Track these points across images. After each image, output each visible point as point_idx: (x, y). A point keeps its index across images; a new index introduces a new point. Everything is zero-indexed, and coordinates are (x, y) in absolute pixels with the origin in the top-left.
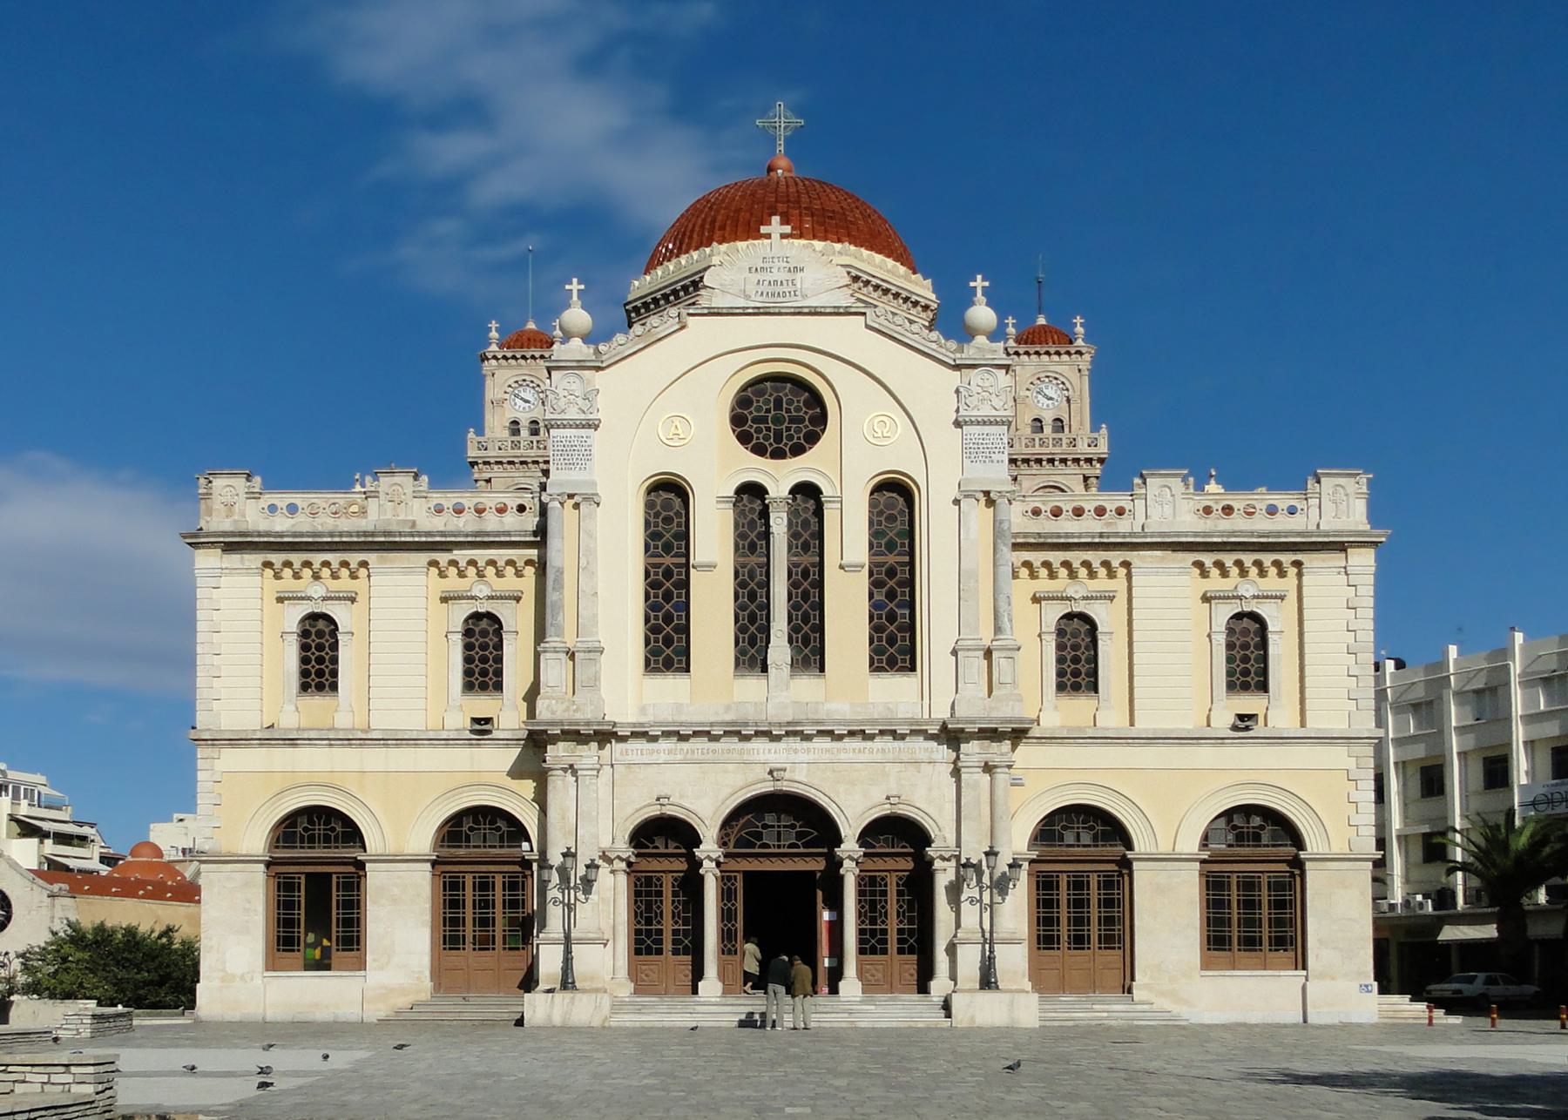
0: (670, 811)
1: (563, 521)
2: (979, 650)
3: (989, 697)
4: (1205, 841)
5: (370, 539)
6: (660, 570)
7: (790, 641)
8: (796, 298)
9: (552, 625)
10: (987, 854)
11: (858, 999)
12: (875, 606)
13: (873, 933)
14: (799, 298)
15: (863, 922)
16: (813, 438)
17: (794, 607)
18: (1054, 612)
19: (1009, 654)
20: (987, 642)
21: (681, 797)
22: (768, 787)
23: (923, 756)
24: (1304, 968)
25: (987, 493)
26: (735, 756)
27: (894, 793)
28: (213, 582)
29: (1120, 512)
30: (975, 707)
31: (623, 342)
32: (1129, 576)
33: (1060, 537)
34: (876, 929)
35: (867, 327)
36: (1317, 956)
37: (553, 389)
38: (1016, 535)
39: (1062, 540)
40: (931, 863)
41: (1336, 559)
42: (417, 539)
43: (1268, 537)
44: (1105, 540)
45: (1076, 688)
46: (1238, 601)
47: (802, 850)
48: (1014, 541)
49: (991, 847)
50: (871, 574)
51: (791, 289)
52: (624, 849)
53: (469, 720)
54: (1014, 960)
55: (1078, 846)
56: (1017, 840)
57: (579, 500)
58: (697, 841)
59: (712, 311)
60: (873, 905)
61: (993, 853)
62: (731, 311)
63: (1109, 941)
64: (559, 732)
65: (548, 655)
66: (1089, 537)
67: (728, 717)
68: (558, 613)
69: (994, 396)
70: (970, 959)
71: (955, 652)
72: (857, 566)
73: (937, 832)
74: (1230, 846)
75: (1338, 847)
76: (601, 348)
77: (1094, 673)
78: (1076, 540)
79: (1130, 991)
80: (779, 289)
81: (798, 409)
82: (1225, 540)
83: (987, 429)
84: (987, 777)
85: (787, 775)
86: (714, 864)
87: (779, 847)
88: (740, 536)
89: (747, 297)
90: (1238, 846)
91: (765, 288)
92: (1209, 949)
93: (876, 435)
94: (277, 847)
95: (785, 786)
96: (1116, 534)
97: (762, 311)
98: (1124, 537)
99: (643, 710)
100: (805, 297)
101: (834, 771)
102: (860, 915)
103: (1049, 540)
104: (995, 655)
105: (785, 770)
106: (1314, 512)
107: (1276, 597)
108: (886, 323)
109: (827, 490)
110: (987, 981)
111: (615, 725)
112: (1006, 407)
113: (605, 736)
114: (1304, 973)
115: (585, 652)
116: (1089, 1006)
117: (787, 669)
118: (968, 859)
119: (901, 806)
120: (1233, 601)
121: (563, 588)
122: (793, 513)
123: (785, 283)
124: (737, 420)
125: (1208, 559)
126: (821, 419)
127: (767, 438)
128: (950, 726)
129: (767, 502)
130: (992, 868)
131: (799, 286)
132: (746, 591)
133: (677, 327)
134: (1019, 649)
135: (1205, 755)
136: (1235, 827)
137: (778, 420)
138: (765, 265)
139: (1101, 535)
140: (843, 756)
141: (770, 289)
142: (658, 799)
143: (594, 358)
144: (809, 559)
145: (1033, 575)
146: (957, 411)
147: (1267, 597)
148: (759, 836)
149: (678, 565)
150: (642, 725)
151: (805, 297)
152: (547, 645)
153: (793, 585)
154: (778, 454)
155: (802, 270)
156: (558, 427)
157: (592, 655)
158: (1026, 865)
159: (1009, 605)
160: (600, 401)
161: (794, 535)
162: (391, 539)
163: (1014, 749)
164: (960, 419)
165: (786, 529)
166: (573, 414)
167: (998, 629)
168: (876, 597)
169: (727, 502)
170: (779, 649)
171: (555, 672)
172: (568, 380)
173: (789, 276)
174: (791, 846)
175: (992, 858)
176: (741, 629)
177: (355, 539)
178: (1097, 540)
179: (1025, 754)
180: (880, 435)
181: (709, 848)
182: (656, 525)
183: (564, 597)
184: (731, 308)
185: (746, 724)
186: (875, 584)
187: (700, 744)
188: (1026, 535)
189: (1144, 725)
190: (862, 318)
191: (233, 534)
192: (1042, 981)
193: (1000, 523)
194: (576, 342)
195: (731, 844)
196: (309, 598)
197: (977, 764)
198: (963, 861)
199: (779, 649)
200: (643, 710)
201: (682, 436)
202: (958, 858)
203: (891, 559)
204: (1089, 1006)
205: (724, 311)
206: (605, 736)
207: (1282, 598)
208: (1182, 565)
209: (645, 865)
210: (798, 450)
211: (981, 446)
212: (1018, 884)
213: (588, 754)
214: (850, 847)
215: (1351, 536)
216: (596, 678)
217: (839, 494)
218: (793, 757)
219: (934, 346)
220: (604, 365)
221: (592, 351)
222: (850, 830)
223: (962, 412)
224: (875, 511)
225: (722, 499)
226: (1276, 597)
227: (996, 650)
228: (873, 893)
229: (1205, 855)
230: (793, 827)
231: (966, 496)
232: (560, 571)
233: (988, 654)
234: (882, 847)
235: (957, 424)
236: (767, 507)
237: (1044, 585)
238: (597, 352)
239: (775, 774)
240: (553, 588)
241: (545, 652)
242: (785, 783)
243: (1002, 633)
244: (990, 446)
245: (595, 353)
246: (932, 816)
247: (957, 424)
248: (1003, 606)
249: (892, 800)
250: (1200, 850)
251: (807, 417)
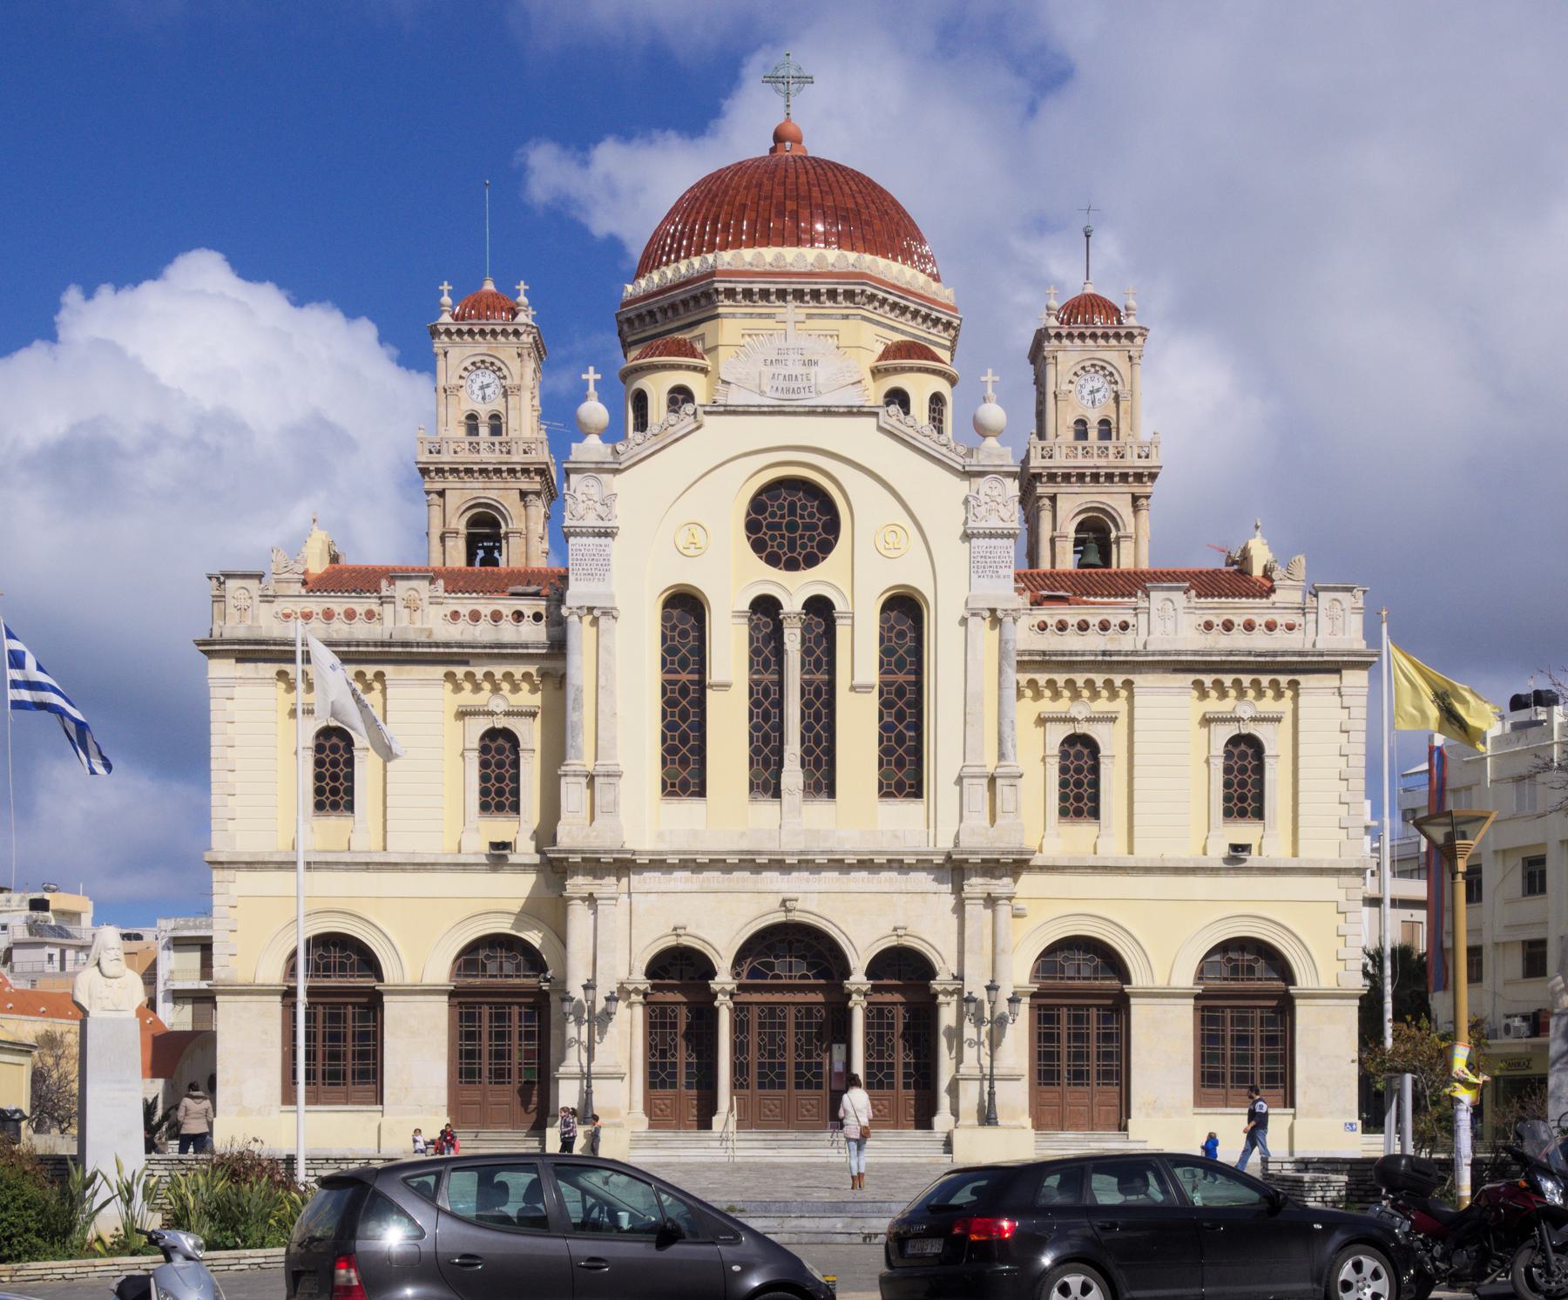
1: (581, 636)
3: (992, 826)
4: (1200, 976)
6: (677, 687)
7: (803, 766)
8: (809, 395)
9: (572, 747)
10: (989, 988)
12: (885, 728)
13: (880, 1067)
14: (813, 395)
15: (870, 1056)
16: (827, 547)
17: (806, 728)
18: (1060, 732)
19: (1012, 781)
20: (990, 770)
22: (780, 917)
25: (993, 611)
27: (901, 925)
29: (1124, 626)
30: (980, 838)
31: (641, 441)
32: (1131, 698)
35: (880, 429)
37: (571, 492)
38: (1021, 653)
40: (935, 996)
45: (1078, 813)
47: (812, 981)
48: (1019, 658)
49: (992, 981)
50: (881, 694)
51: (806, 384)
52: (640, 980)
54: (1015, 1097)
55: (1079, 978)
56: (1019, 973)
57: (597, 614)
58: (711, 972)
59: (728, 408)
60: (880, 1036)
61: (992, 988)
62: (746, 409)
63: (1106, 1075)
64: (579, 860)
65: (569, 779)
66: (1092, 655)
67: (745, 846)
68: (578, 734)
69: (1001, 506)
70: (970, 1096)
71: (960, 780)
73: (942, 965)
76: (620, 447)
77: (1095, 798)
78: (1079, 658)
79: (1126, 1129)
80: (794, 385)
81: (811, 515)
83: (993, 542)
84: (989, 912)
85: (799, 905)
86: (728, 997)
87: (790, 977)
88: (755, 652)
89: (762, 393)
91: (781, 383)
92: (1203, 1086)
93: (887, 546)
95: (797, 917)
96: (1119, 653)
97: (776, 409)
98: (1126, 655)
99: (660, 836)
100: (819, 393)
102: (867, 1047)
103: (1054, 658)
104: (999, 782)
105: (796, 900)
108: (898, 425)
109: (840, 606)
110: (987, 1116)
111: (634, 853)
112: (1013, 518)
113: (624, 866)
114: (1292, 1111)
115: (604, 776)
118: (970, 993)
119: (907, 938)
122: (806, 629)
123: (799, 378)
124: (752, 527)
126: (833, 526)
127: (781, 546)
128: (954, 857)
129: (781, 617)
130: (993, 1003)
131: (813, 381)
132: (760, 711)
133: (694, 426)
134: (1021, 776)
137: (792, 527)
138: (780, 357)
139: (1104, 653)
141: (785, 384)
142: (675, 929)
143: (611, 459)
144: (821, 677)
145: (1038, 695)
146: (966, 522)
148: (771, 967)
149: (692, 682)
150: (661, 853)
151: (819, 393)
152: (567, 768)
153: (806, 705)
154: (792, 565)
155: (816, 363)
156: (582, 534)
157: (610, 780)
158: (1026, 1000)
159: (1013, 729)
160: (618, 507)
161: (806, 651)
163: (1015, 882)
164: (969, 531)
165: (799, 647)
166: (591, 521)
167: (1002, 756)
169: (743, 617)
170: (793, 775)
171: (573, 795)
172: (585, 483)
173: (804, 370)
174: (802, 977)
175: (993, 993)
176: (755, 751)
178: (1100, 658)
179: (1028, 883)
180: (891, 546)
181: (724, 979)
183: (582, 717)
184: (749, 406)
185: (760, 853)
186: (885, 704)
188: (1031, 653)
189: (1145, 853)
190: (873, 420)
192: (1044, 1118)
193: (1006, 643)
194: (593, 440)
195: (744, 974)
198: (966, 995)
199: (793, 775)
200: (660, 836)
201: (698, 546)
202: (959, 992)
203: (901, 678)
205: (740, 409)
206: (624, 866)
209: (660, 997)
210: (811, 561)
211: (988, 560)
212: (1018, 1019)
213: (607, 886)
214: (858, 979)
216: (615, 803)
217: (850, 610)
218: (805, 887)
219: (944, 450)
220: (622, 467)
221: (609, 450)
222: (859, 964)
223: (971, 524)
225: (738, 614)
228: (880, 1026)
229: (1199, 990)
231: (973, 615)
232: (580, 690)
233: (992, 780)
235: (967, 536)
236: (781, 622)
237: (1047, 706)
238: (616, 452)
239: (788, 904)
240: (574, 708)
242: (797, 913)
243: (1005, 759)
245: (612, 454)
246: (937, 947)
247: (967, 536)
248: (1007, 729)
249: (900, 932)
250: (1195, 984)
251: (820, 524)
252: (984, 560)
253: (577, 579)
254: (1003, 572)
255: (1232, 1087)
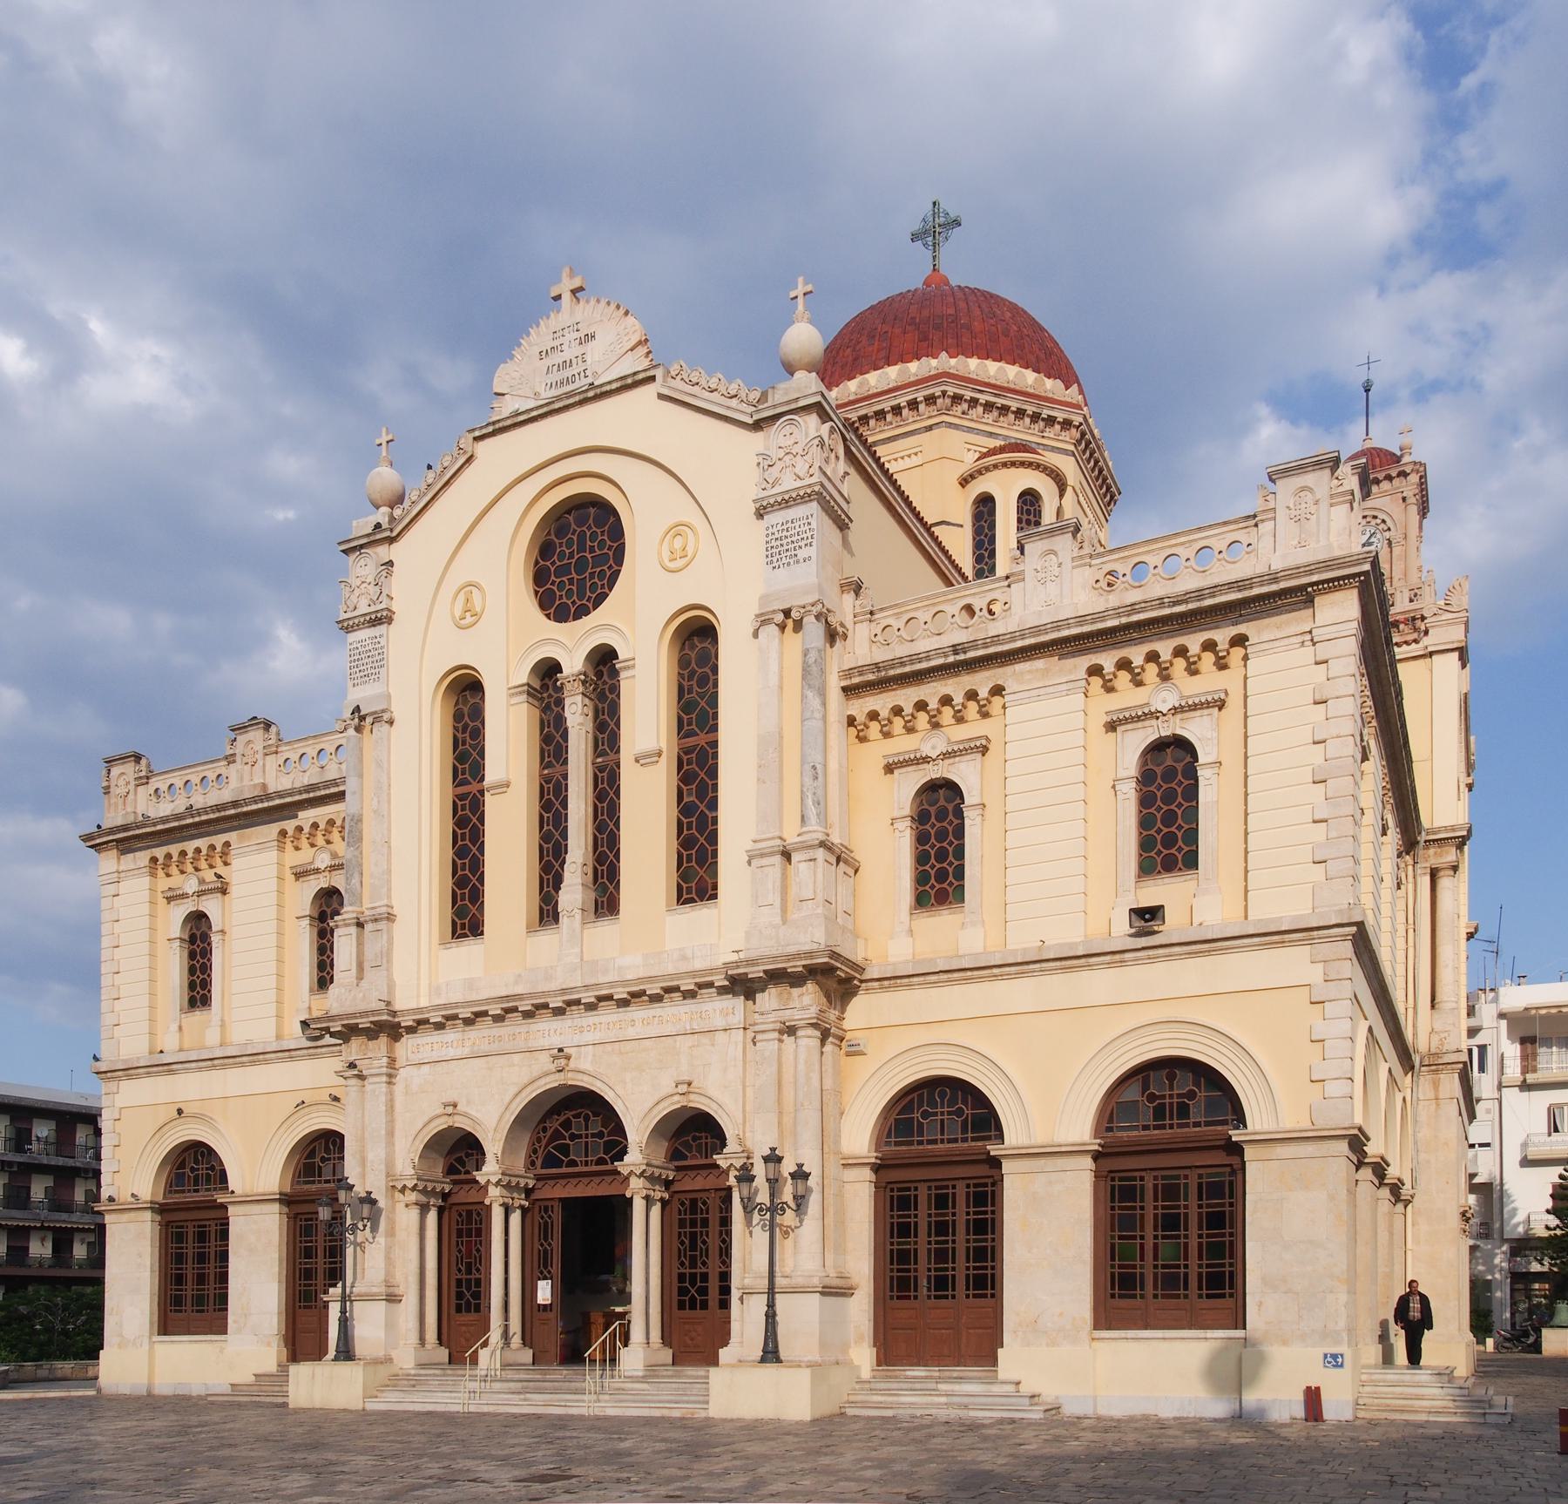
0: (461, 1123)
2: (772, 854)
3: (784, 923)
5: (223, 814)
11: (641, 1374)
21: (468, 1102)
23: (720, 1023)
24: (1245, 1329)
26: (522, 1045)
28: (112, 889)
33: (903, 664)
34: (696, 1273)
36: (1260, 1304)
39: (907, 669)
41: (1295, 622)
42: (260, 806)
43: (1186, 602)
44: (961, 657)
46: (1154, 722)
53: (299, 1025)
72: (649, 756)
74: (1146, 1128)
75: (1292, 1119)
82: (1124, 620)
90: (1156, 1127)
94: (170, 1192)
98: (985, 646)
101: (621, 1053)
103: (892, 673)
106: (1266, 542)
107: (1207, 705)
116: (933, 1386)
117: (578, 915)
120: (1147, 723)
121: (361, 839)
125: (1107, 660)
135: (1098, 983)
136: (1152, 1098)
137: (581, 566)
140: (631, 1033)
147: (1194, 707)
148: (565, 1150)
162: (239, 810)
168: (686, 799)
170: (574, 891)
172: (359, 565)
177: (212, 816)
178: (951, 659)
182: (464, 743)
187: (483, 1034)
191: (125, 828)
195: (539, 1163)
196: (184, 896)
197: (771, 1026)
199: (574, 891)
204: (933, 1386)
207: (1221, 705)
208: (1073, 677)
215: (1311, 572)
220: (394, 534)
224: (685, 672)
226: (1207, 705)
227: (796, 850)
228: (693, 1223)
230: (600, 1135)
234: (694, 1157)
241: (337, 926)
242: (570, 1075)
244: (794, 539)
252: (778, 543)
253: (354, 685)
254: (802, 554)
255: (1155, 1296)
